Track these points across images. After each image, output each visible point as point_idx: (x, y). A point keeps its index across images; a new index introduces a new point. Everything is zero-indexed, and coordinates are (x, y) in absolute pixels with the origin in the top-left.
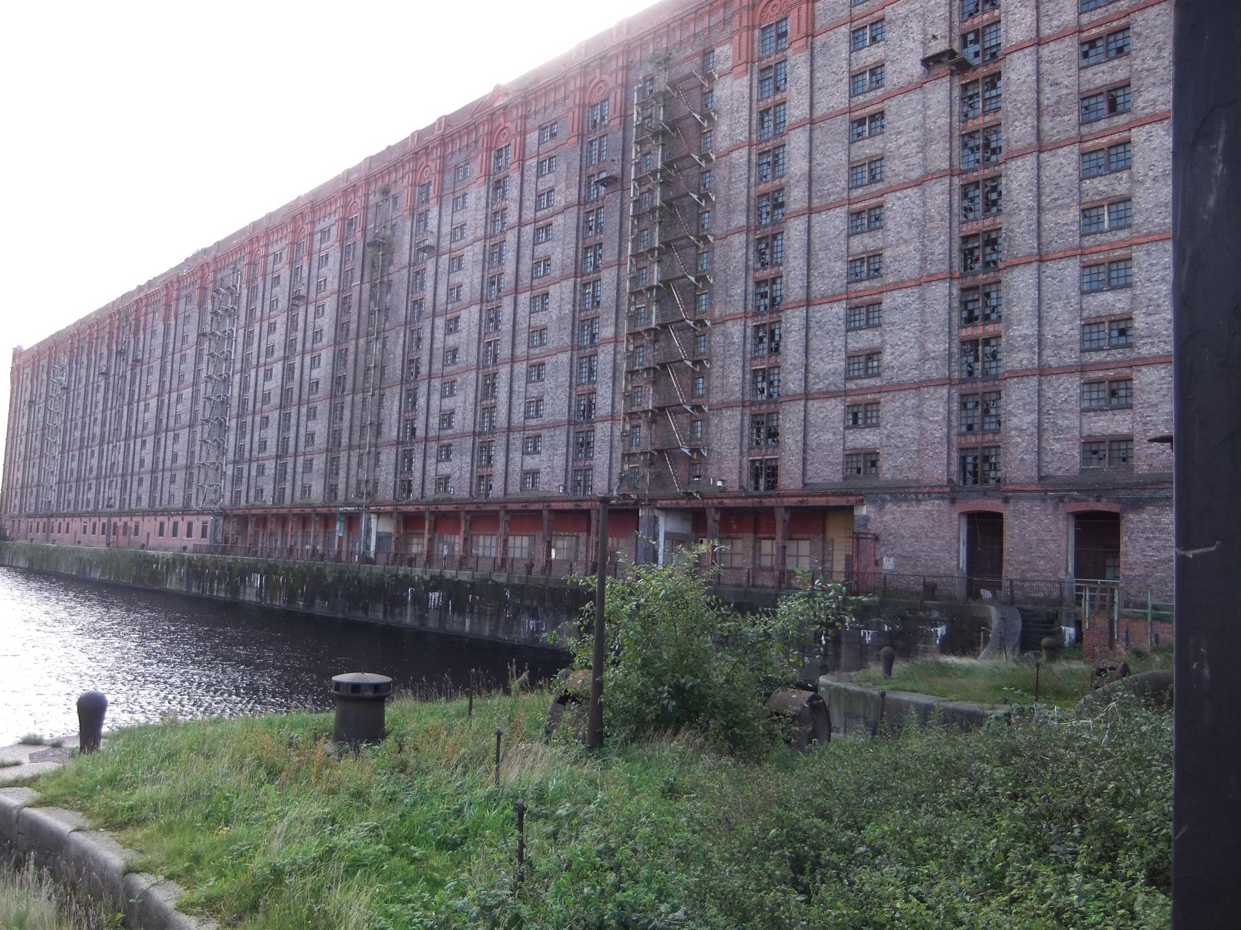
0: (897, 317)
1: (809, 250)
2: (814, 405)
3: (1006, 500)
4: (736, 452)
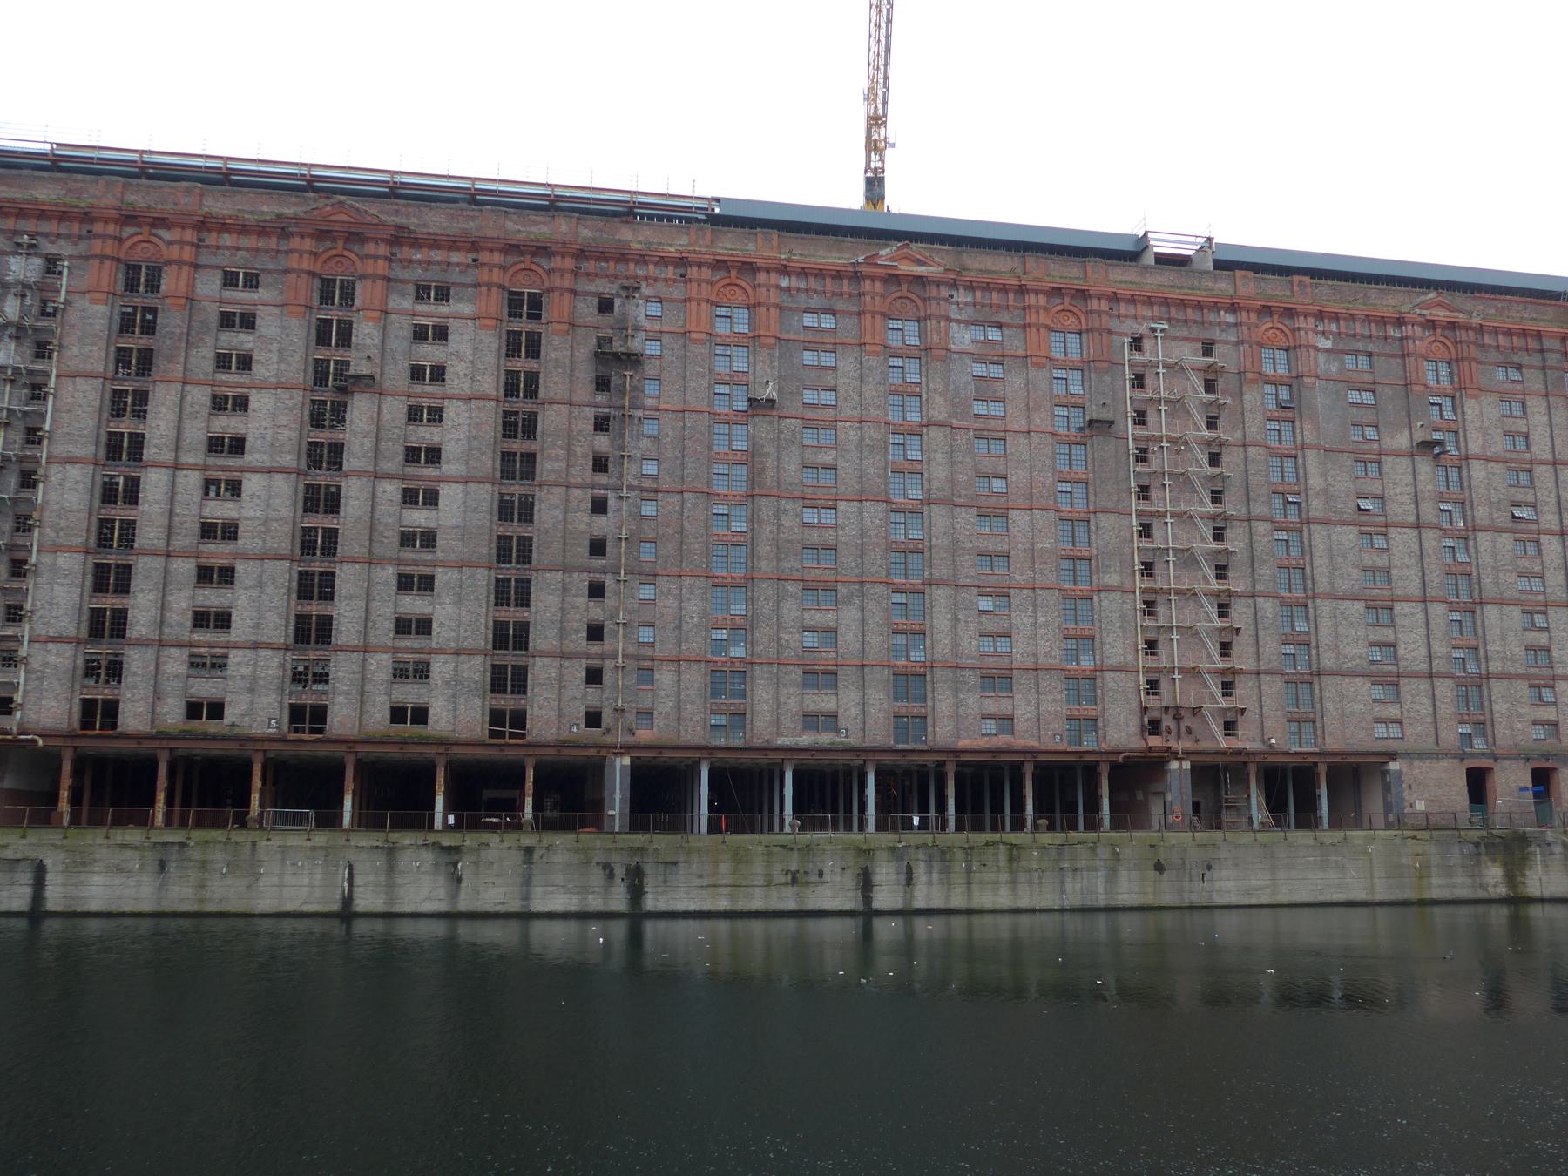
0: (1406, 622)
3: (1496, 760)
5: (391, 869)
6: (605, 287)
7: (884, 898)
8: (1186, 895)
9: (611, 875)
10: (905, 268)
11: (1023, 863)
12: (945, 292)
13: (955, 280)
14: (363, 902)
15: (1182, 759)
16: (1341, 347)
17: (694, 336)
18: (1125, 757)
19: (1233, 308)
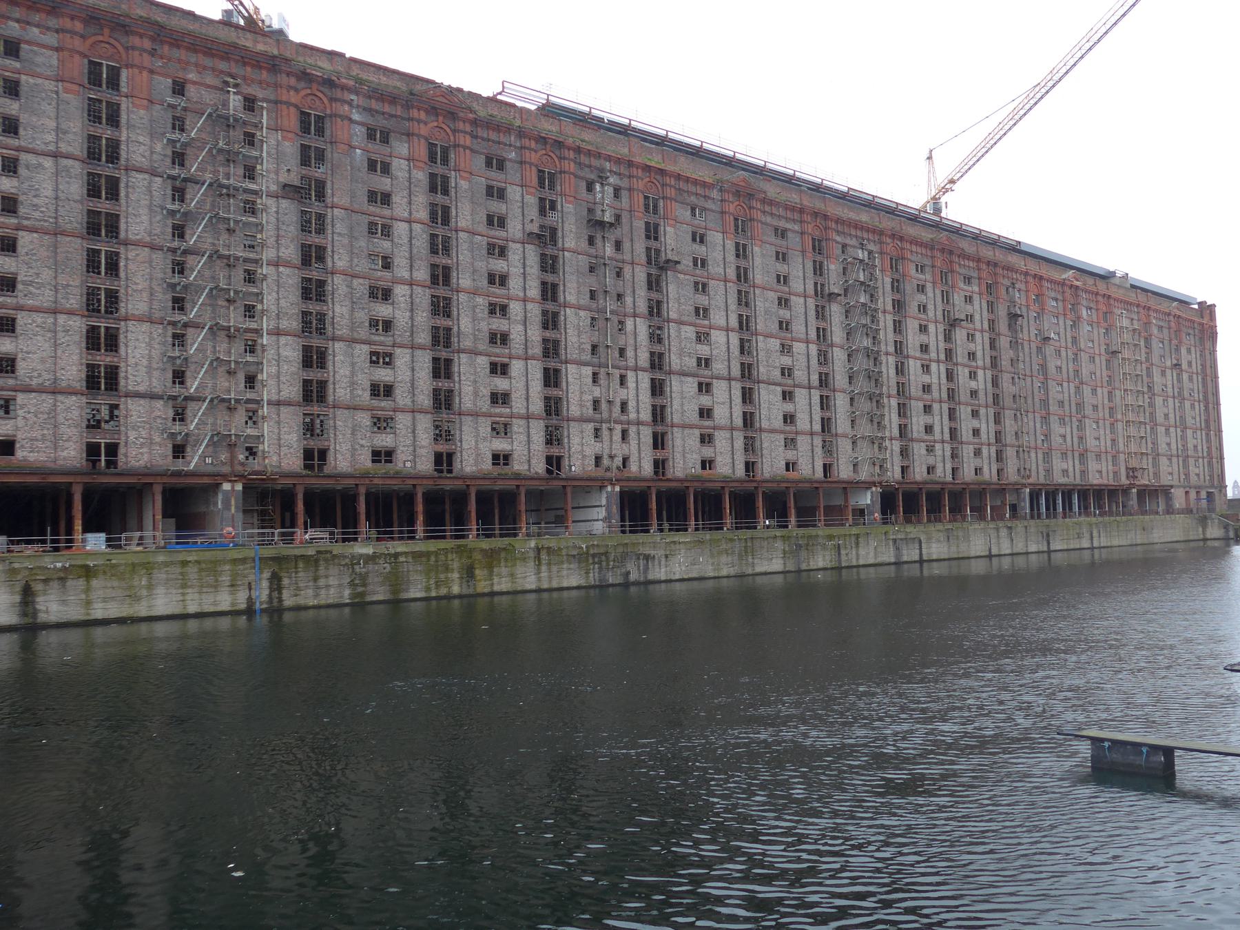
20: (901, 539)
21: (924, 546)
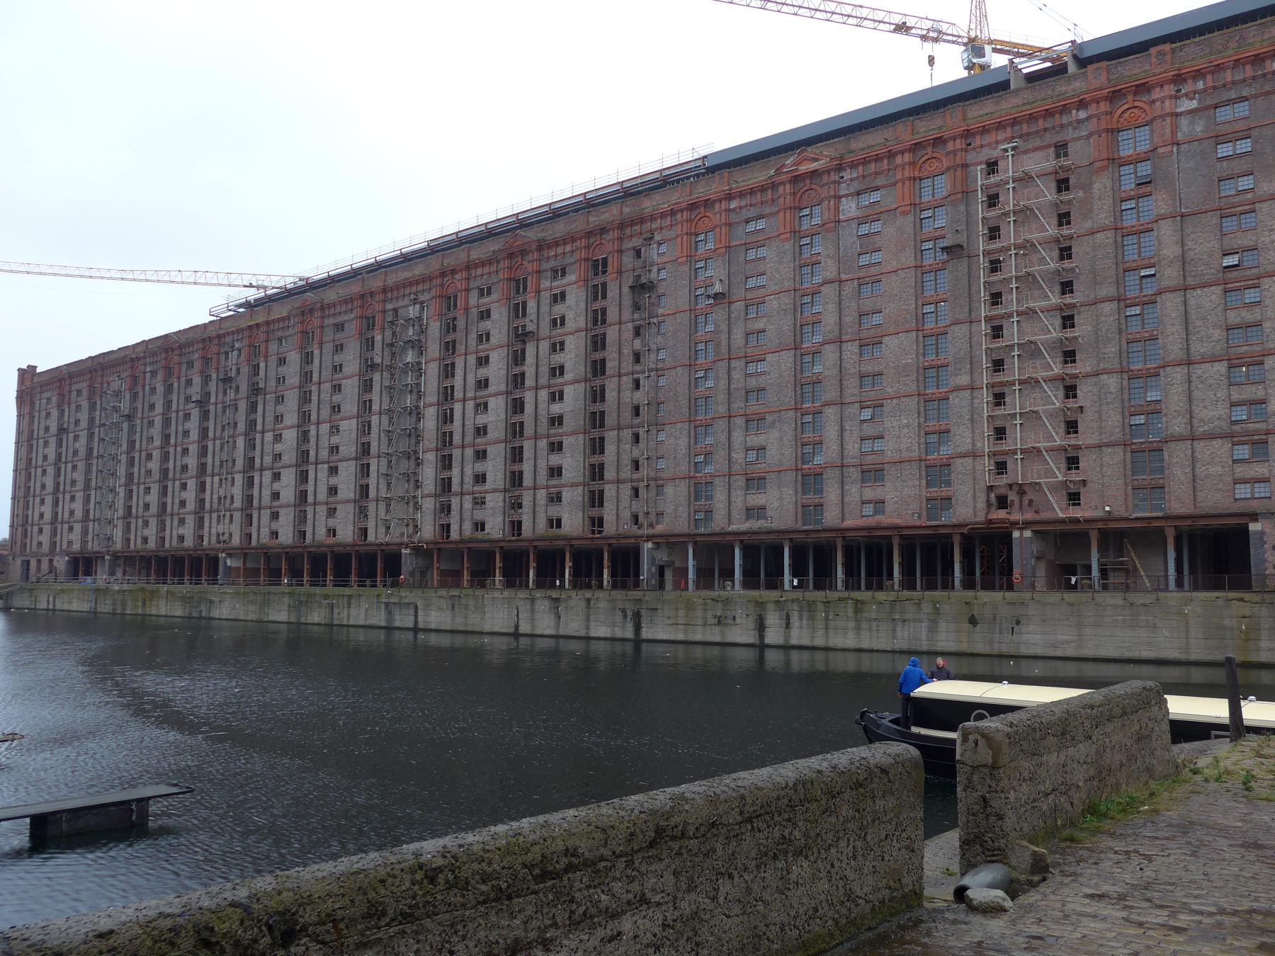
1: (1186, 319)
2: (1199, 445)
4: (1121, 482)
5: (533, 610)
6: (636, 242)
7: (772, 637)
8: (996, 646)
9: (625, 617)
10: (805, 167)
11: (865, 615)
12: (834, 177)
13: (840, 165)
14: (524, 628)
15: (1023, 529)
16: (1209, 102)
17: (680, 260)
18: (972, 529)
19: (1082, 105)
20: (394, 604)
21: (420, 612)
